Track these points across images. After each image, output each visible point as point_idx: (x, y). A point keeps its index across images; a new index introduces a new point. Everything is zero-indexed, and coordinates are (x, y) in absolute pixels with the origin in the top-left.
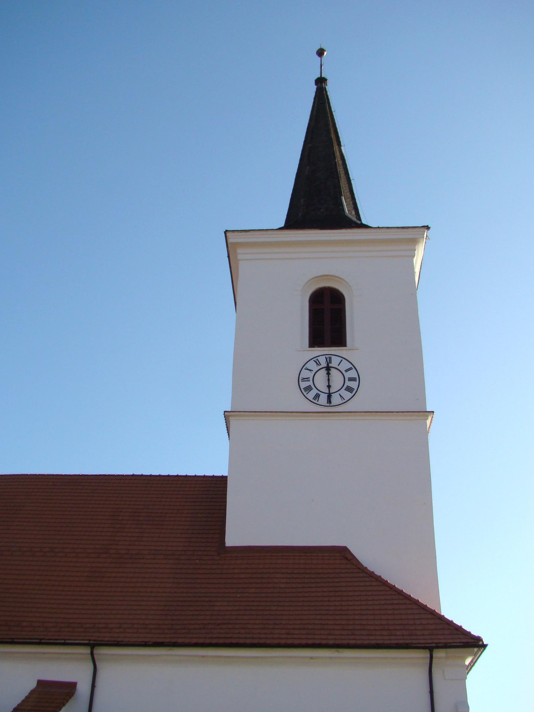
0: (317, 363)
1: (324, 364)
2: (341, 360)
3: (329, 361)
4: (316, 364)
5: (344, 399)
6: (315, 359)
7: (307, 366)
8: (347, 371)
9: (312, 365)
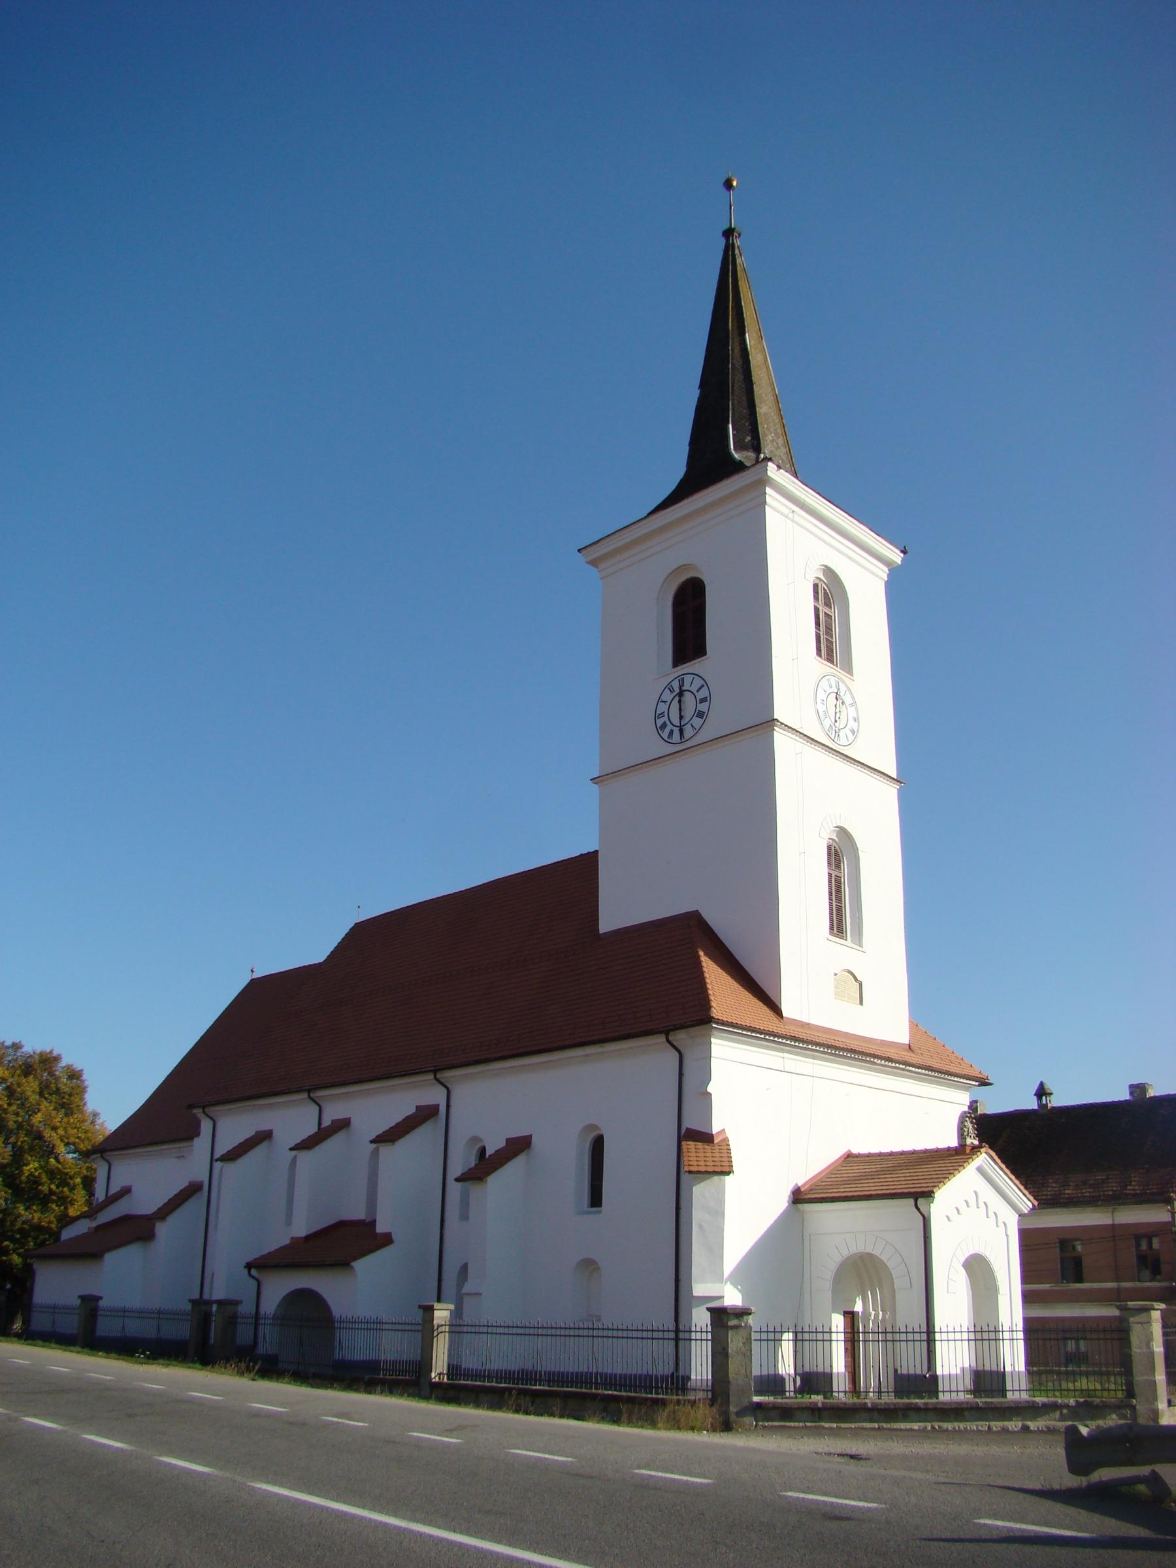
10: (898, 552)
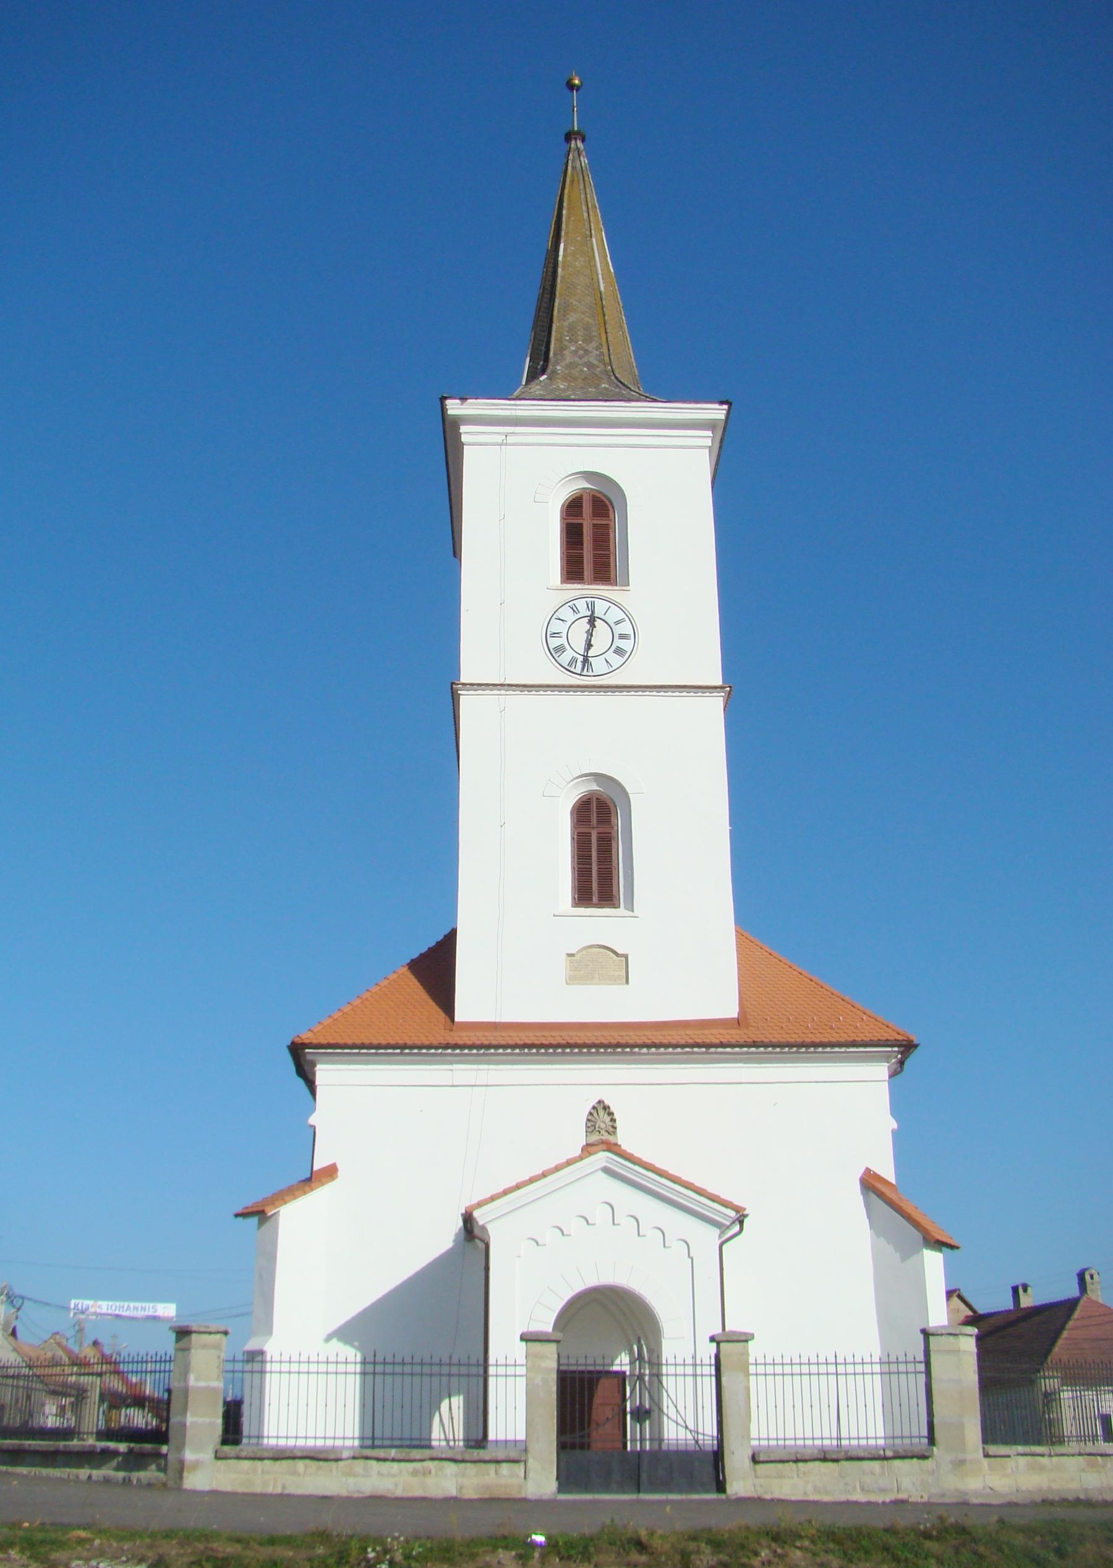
0: (574, 611)
2: (608, 607)
3: (592, 607)
4: (572, 611)
5: (612, 666)
8: (617, 623)
9: (566, 613)
10: (717, 406)
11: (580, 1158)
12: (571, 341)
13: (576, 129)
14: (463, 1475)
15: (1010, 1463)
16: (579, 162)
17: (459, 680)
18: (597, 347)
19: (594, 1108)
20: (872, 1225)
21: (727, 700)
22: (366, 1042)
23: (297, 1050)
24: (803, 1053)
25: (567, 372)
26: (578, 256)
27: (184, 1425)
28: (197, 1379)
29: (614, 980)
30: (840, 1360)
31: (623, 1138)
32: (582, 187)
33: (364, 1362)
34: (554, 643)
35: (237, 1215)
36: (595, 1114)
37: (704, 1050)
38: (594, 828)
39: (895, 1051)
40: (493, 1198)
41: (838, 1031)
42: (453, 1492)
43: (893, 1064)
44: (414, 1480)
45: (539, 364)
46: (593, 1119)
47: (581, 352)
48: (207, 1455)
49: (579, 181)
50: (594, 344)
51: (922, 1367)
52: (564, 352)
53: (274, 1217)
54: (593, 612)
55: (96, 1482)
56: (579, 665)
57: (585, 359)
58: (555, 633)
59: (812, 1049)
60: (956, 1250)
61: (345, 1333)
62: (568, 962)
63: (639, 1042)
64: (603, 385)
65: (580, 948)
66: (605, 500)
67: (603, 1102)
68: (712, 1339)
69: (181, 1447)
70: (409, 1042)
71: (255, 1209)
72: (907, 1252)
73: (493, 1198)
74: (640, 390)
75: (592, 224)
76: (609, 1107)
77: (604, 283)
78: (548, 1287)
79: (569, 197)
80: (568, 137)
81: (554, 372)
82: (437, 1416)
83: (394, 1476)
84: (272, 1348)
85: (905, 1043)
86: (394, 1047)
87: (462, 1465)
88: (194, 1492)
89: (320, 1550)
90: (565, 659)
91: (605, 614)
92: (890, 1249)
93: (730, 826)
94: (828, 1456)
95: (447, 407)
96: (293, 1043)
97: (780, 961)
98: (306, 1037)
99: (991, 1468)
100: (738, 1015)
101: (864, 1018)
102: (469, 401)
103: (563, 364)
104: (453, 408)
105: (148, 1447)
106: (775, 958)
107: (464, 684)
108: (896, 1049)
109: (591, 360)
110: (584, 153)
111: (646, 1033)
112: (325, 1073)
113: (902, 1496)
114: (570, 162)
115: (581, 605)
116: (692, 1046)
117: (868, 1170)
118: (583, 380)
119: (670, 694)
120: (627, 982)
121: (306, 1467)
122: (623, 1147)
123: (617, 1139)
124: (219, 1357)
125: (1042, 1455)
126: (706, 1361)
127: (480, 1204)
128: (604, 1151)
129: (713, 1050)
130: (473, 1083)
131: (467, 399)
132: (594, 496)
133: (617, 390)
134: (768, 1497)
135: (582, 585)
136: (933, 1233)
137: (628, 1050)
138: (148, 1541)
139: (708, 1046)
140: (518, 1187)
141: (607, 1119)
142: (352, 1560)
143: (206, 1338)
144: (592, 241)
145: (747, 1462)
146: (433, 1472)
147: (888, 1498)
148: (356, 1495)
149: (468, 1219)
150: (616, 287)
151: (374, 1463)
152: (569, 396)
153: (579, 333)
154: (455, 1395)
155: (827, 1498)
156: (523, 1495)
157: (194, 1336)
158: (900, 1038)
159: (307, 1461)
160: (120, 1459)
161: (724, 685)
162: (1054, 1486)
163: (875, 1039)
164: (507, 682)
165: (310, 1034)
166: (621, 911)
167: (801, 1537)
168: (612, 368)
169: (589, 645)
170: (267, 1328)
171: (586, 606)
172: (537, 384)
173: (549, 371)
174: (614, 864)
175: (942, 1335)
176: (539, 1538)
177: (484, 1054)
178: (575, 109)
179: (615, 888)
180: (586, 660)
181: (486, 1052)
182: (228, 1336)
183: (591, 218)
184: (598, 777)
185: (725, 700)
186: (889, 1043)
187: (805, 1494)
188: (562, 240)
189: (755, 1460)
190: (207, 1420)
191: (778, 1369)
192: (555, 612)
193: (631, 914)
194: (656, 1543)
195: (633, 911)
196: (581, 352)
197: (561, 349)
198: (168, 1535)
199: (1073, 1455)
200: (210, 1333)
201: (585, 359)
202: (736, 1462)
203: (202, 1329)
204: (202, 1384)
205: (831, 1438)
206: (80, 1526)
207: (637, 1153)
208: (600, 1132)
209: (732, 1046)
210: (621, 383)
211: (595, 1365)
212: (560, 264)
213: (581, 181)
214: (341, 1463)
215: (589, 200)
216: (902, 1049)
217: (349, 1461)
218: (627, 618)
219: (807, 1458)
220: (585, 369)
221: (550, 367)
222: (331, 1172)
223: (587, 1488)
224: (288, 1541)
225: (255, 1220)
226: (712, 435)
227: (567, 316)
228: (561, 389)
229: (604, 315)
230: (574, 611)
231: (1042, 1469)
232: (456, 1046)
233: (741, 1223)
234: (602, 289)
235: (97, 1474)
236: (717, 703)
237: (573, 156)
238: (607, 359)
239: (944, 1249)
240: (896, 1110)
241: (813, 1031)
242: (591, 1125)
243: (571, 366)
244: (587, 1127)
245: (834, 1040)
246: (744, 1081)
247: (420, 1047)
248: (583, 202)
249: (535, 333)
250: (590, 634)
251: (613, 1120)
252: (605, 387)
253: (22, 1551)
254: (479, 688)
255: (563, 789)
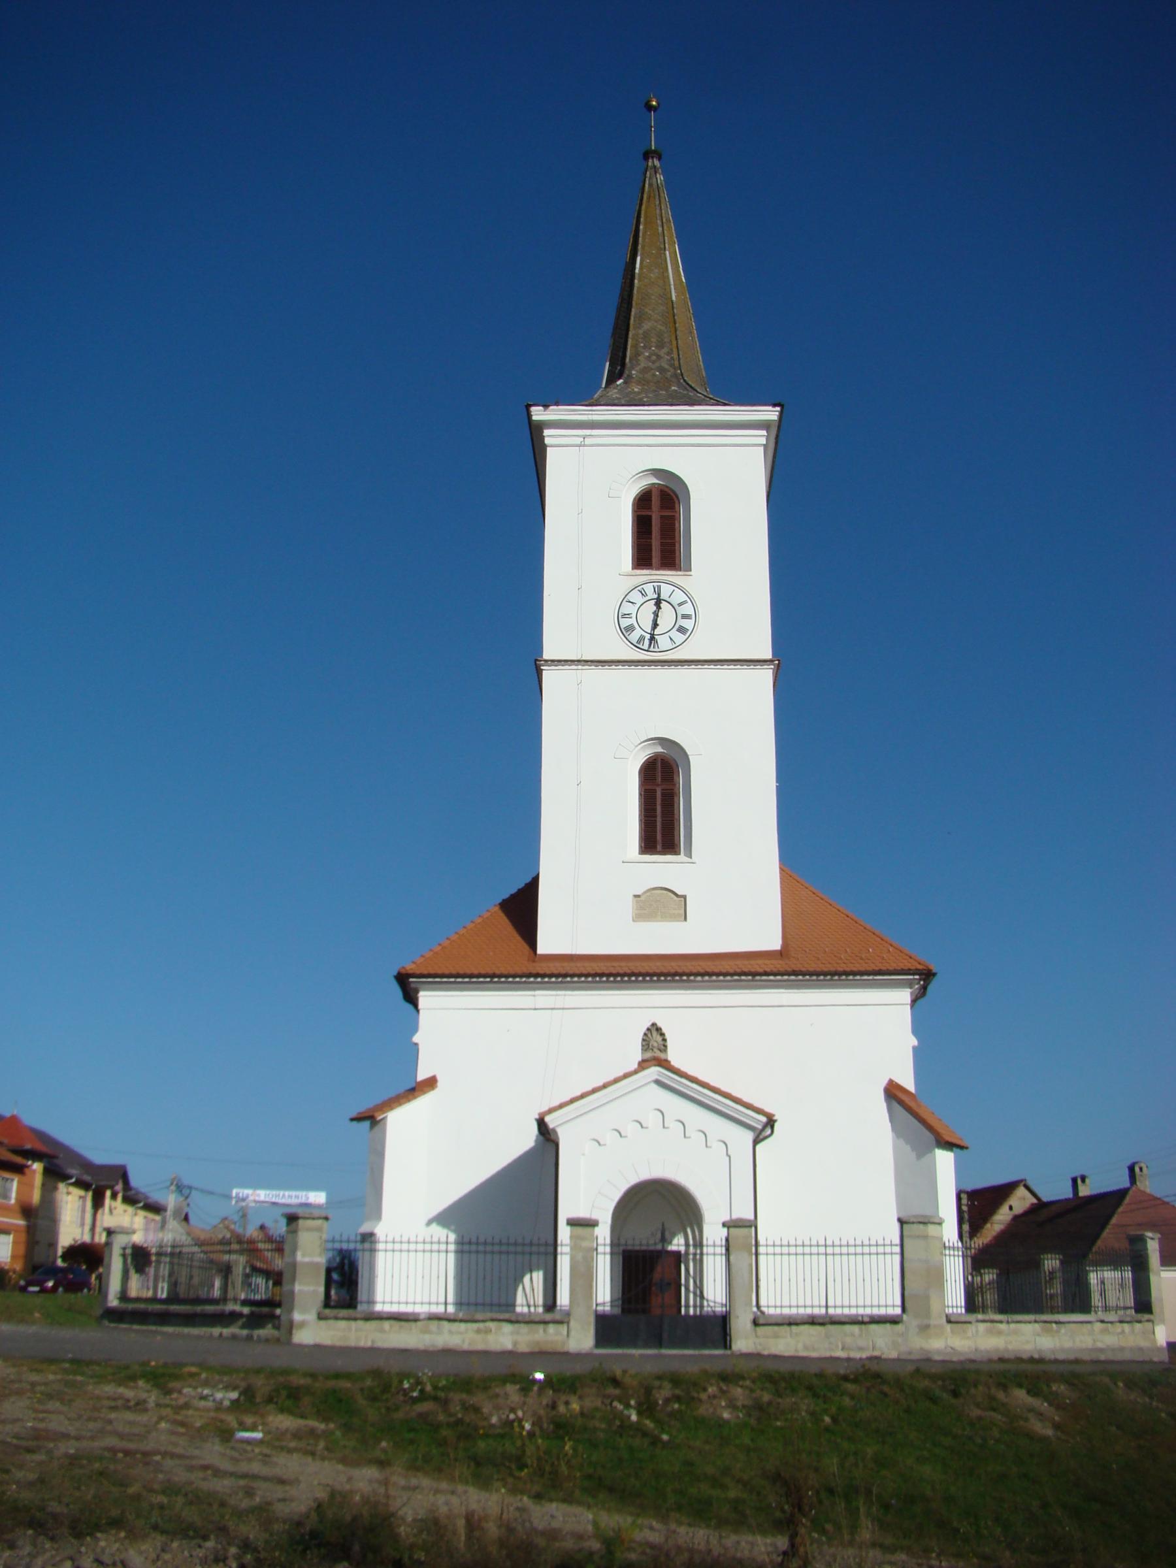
0: (643, 594)
1: (652, 595)
4: (641, 594)
5: (675, 643)
6: (639, 588)
7: (630, 597)
8: (680, 604)
9: (636, 597)
10: (770, 408)
11: (636, 1072)
12: (644, 347)
13: (653, 148)
14: (518, 1333)
15: (971, 1329)
16: (655, 180)
17: (542, 657)
18: (668, 352)
19: (648, 1029)
20: (894, 1129)
21: (777, 671)
22: (461, 972)
23: (402, 979)
24: (843, 980)
25: (641, 376)
26: (653, 268)
27: (292, 1293)
28: (303, 1255)
29: (673, 918)
30: (829, 1242)
31: (674, 1056)
32: (657, 203)
33: (457, 1243)
34: (625, 623)
35: (352, 1120)
36: (649, 1035)
37: (750, 978)
38: (659, 785)
39: (916, 979)
40: (561, 1106)
41: (867, 961)
42: (509, 1346)
43: (917, 988)
44: (479, 1337)
45: (616, 369)
46: (647, 1039)
47: (654, 358)
48: (311, 1316)
49: (655, 198)
50: (665, 350)
51: (897, 1249)
52: (639, 358)
53: (383, 1121)
54: (659, 595)
55: (227, 1338)
56: (647, 642)
57: (657, 364)
58: (625, 615)
59: (844, 977)
60: (965, 1150)
61: (444, 1218)
62: (635, 902)
63: (695, 971)
64: (673, 388)
65: (645, 889)
66: (672, 494)
67: (656, 1024)
68: (724, 1225)
69: (290, 1310)
70: (498, 972)
71: (366, 1115)
72: (922, 1152)
73: (561, 1106)
74: (707, 391)
75: (666, 238)
76: (661, 1029)
77: (675, 292)
78: (608, 1181)
79: (646, 212)
80: (647, 155)
81: (630, 376)
82: (520, 1288)
83: (461, 1333)
84: (382, 1230)
85: (924, 971)
86: (485, 976)
87: (517, 1325)
88: (301, 1346)
89: (369, 1382)
90: (635, 636)
91: (670, 597)
92: (908, 1148)
93: (777, 782)
94: (816, 1321)
95: (532, 413)
96: (399, 973)
97: (822, 899)
98: (410, 967)
99: (952, 1332)
100: (781, 947)
101: (891, 950)
102: (551, 408)
103: (638, 368)
104: (536, 415)
105: (265, 1310)
106: (818, 896)
107: (546, 661)
108: (917, 977)
109: (663, 364)
110: (660, 170)
111: (701, 963)
112: (426, 998)
113: (876, 1353)
114: (647, 179)
115: (649, 589)
116: (740, 974)
117: (891, 1082)
118: (655, 383)
119: (725, 667)
120: (685, 919)
121: (391, 1326)
122: (672, 1063)
123: (667, 1056)
124: (321, 1238)
125: (1001, 1322)
126: (718, 1242)
127: (551, 1111)
128: (655, 1065)
129: (758, 978)
130: (553, 1007)
131: (549, 406)
132: (662, 491)
133: (685, 392)
134: (766, 1353)
135: (651, 571)
136: (944, 1136)
137: (685, 978)
138: (242, 1375)
139: (754, 974)
140: (582, 1096)
141: (659, 1039)
142: (393, 1390)
143: (310, 1223)
144: (665, 254)
145: (749, 1325)
146: (493, 1330)
147: (864, 1355)
148: (431, 1349)
149: (541, 1124)
150: (688, 296)
151: (445, 1323)
152: (641, 399)
153: (652, 340)
154: (535, 1270)
155: (814, 1354)
156: (565, 1349)
157: (301, 1222)
158: (920, 967)
159: (392, 1322)
160: (244, 1320)
161: (774, 659)
162: (1010, 1347)
163: (906, 968)
164: (584, 658)
165: (413, 966)
166: (682, 857)
167: (743, 1378)
168: (681, 372)
169: (655, 625)
170: (377, 1214)
171: (653, 590)
172: (614, 388)
173: (625, 375)
174: (676, 817)
175: (913, 1223)
176: (539, 1376)
177: (561, 982)
178: (653, 129)
179: (676, 838)
180: (652, 638)
181: (563, 980)
182: (329, 1222)
183: (665, 232)
184: (663, 741)
185: (775, 671)
186: (911, 972)
187: (796, 1350)
188: (639, 253)
189: (756, 1323)
190: (312, 1288)
191: (807, 1250)
192: (626, 596)
193: (689, 860)
194: (627, 1380)
195: (691, 858)
196: (654, 358)
197: (637, 354)
198: (258, 1371)
199: (1030, 1322)
200: (314, 1219)
201: (657, 364)
202: (741, 1325)
203: (307, 1216)
204: (307, 1259)
205: (820, 1306)
206: (193, 1365)
207: (684, 1069)
208: (652, 1050)
209: (775, 974)
210: (688, 384)
211: (641, 1245)
212: (637, 276)
213: (657, 197)
214: (419, 1323)
215: (664, 215)
216: (924, 977)
217: (425, 1322)
218: (689, 600)
219: (799, 1322)
220: (657, 373)
221: (627, 372)
222: (431, 1083)
223: (619, 1345)
224: (348, 1376)
225: (367, 1124)
226: (766, 434)
227: (643, 324)
228: (635, 392)
229: (675, 323)
230: (643, 594)
231: (1000, 1333)
232: (536, 975)
233: (772, 1127)
234: (674, 298)
235: (226, 1331)
236: (766, 676)
237: (650, 174)
238: (676, 363)
239: (954, 1149)
240: (918, 1028)
241: (846, 961)
242: (646, 1044)
243: (646, 370)
244: (643, 1046)
245: (870, 969)
246: (785, 1004)
247: (507, 976)
248: (658, 218)
249: (614, 340)
250: (656, 615)
251: (665, 1040)
252: (674, 390)
253: (148, 1381)
254: (559, 663)
255: (631, 752)
